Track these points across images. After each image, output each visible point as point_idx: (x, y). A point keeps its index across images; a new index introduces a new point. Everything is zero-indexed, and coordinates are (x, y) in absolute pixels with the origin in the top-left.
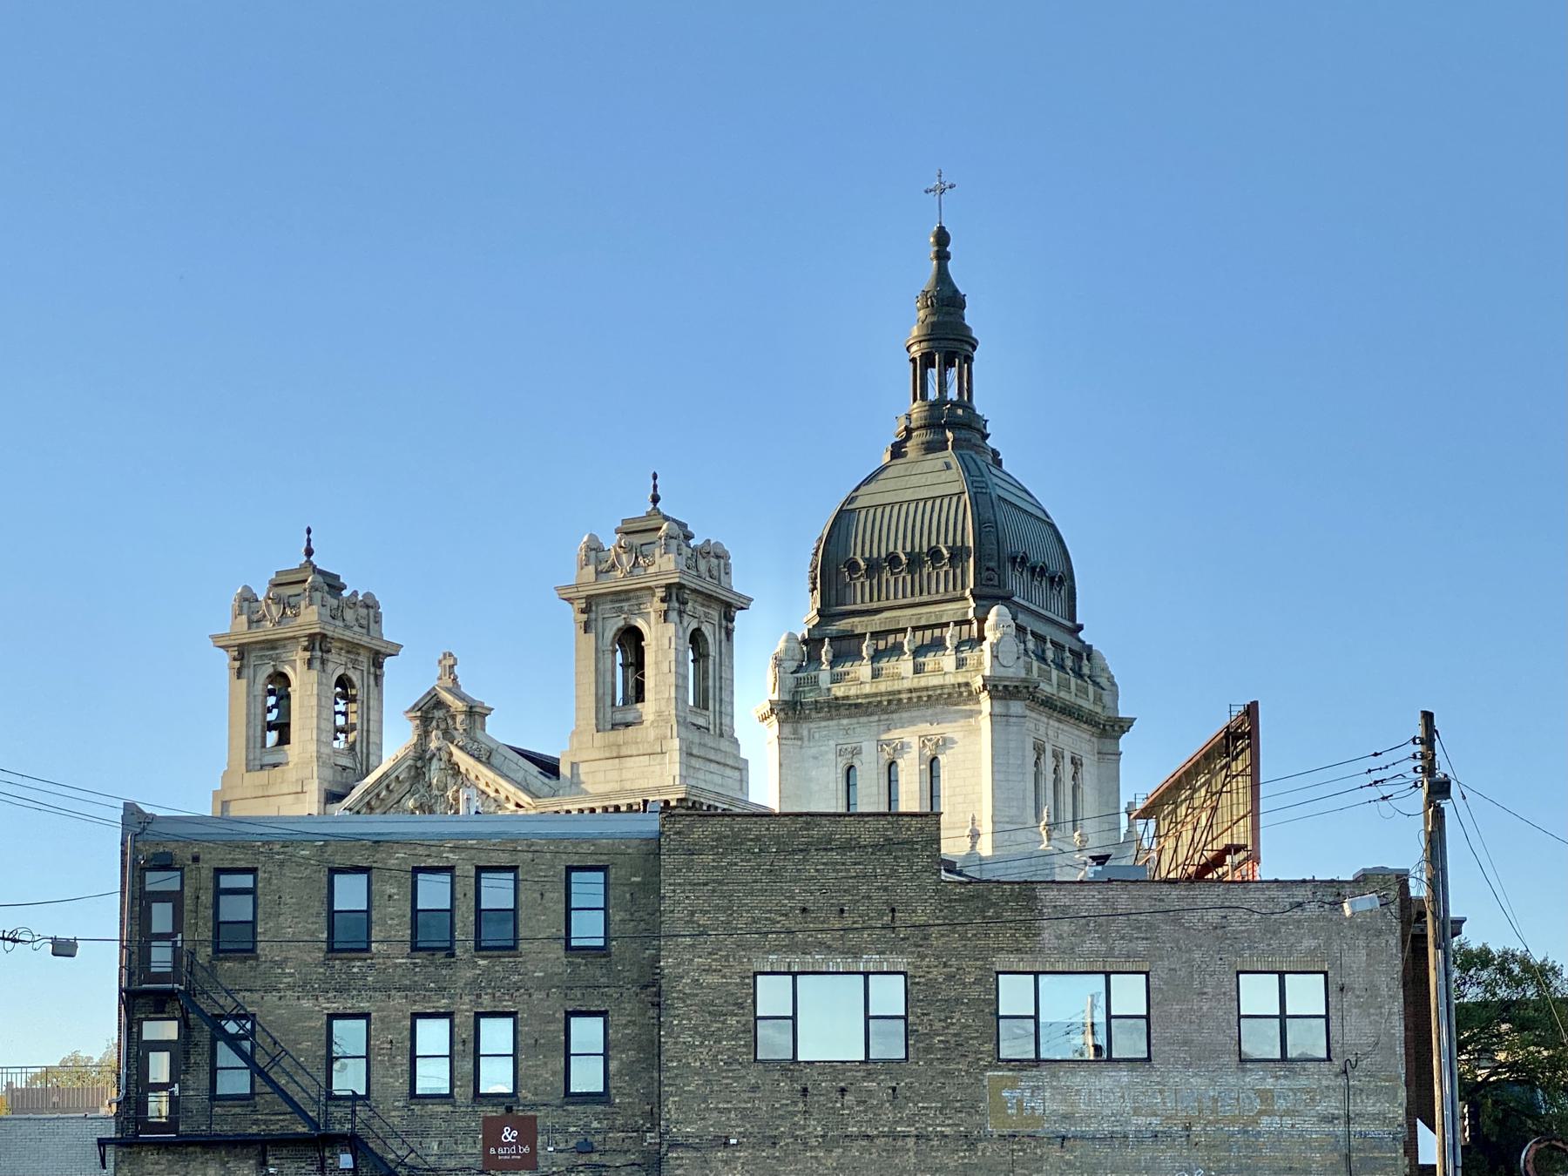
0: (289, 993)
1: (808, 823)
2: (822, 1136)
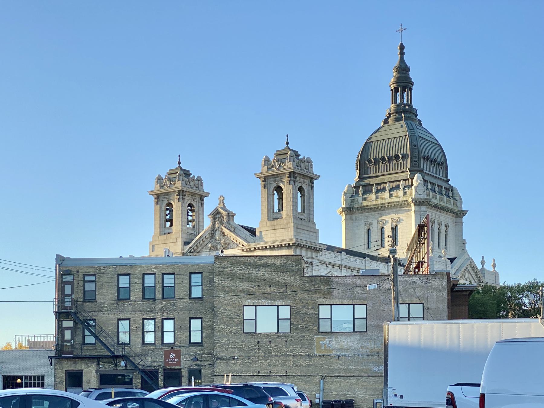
0: (106, 312)
2: (264, 356)
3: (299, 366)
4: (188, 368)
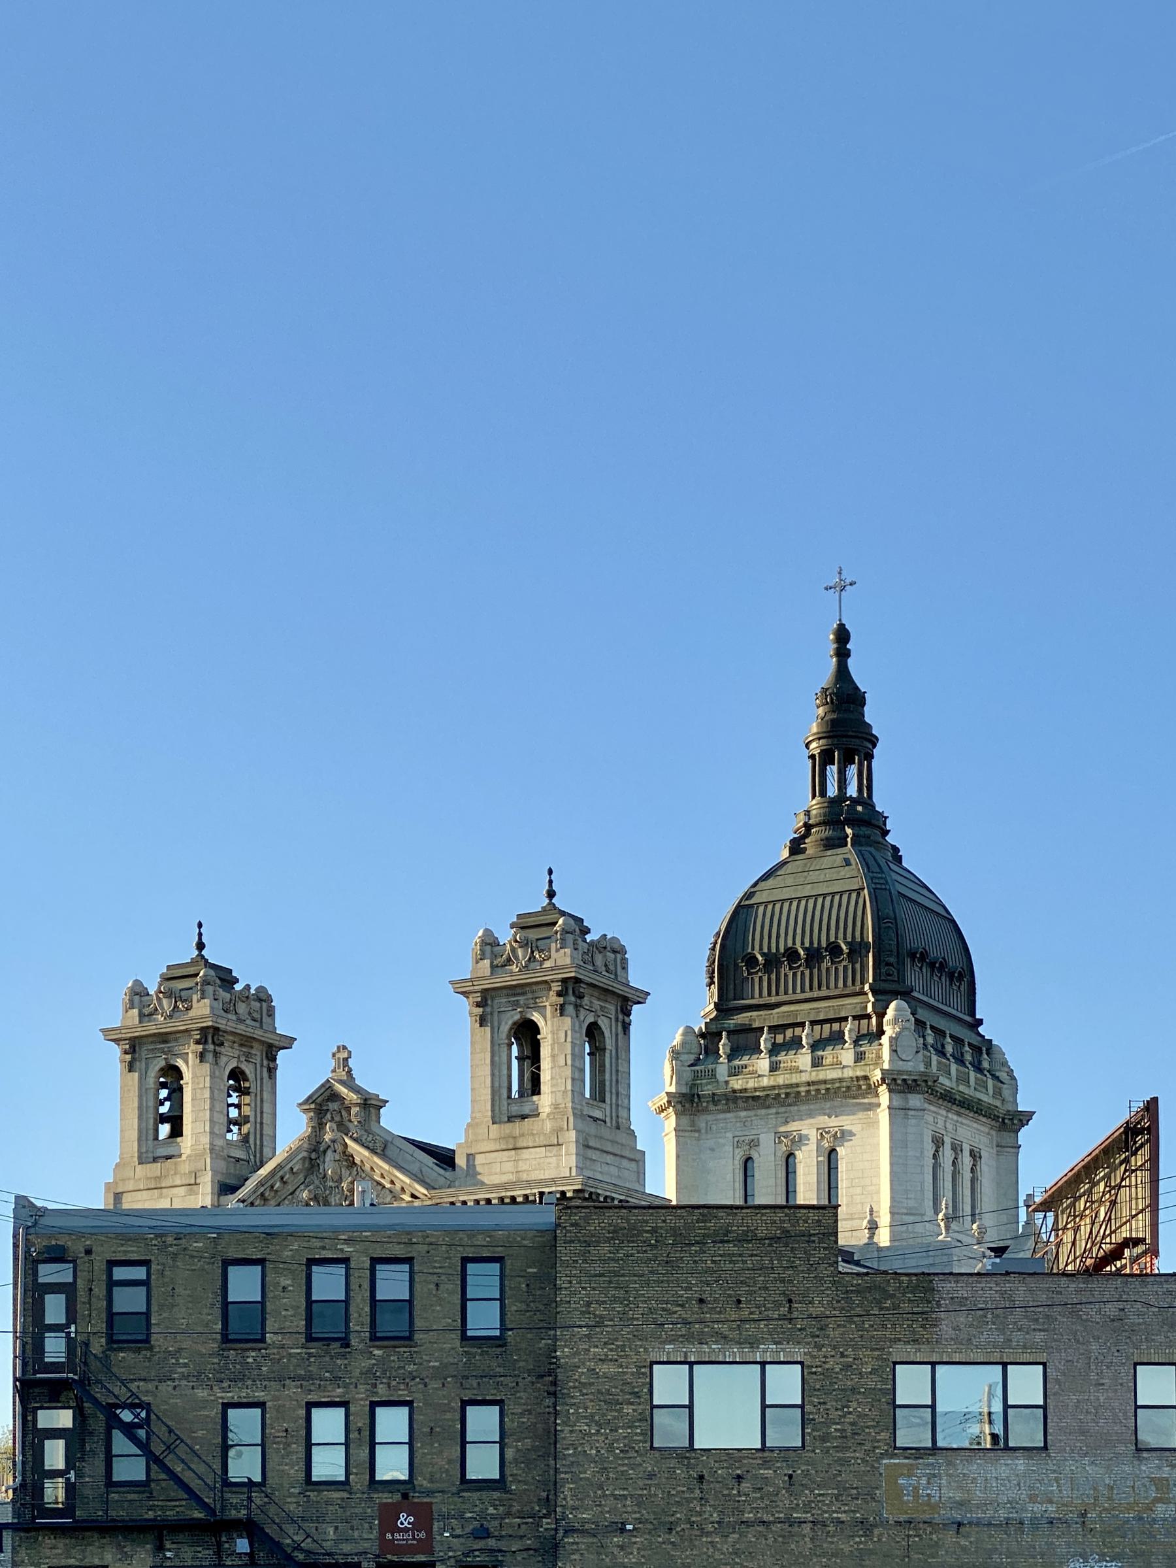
2: (718, 1522)
4: (456, 1561)
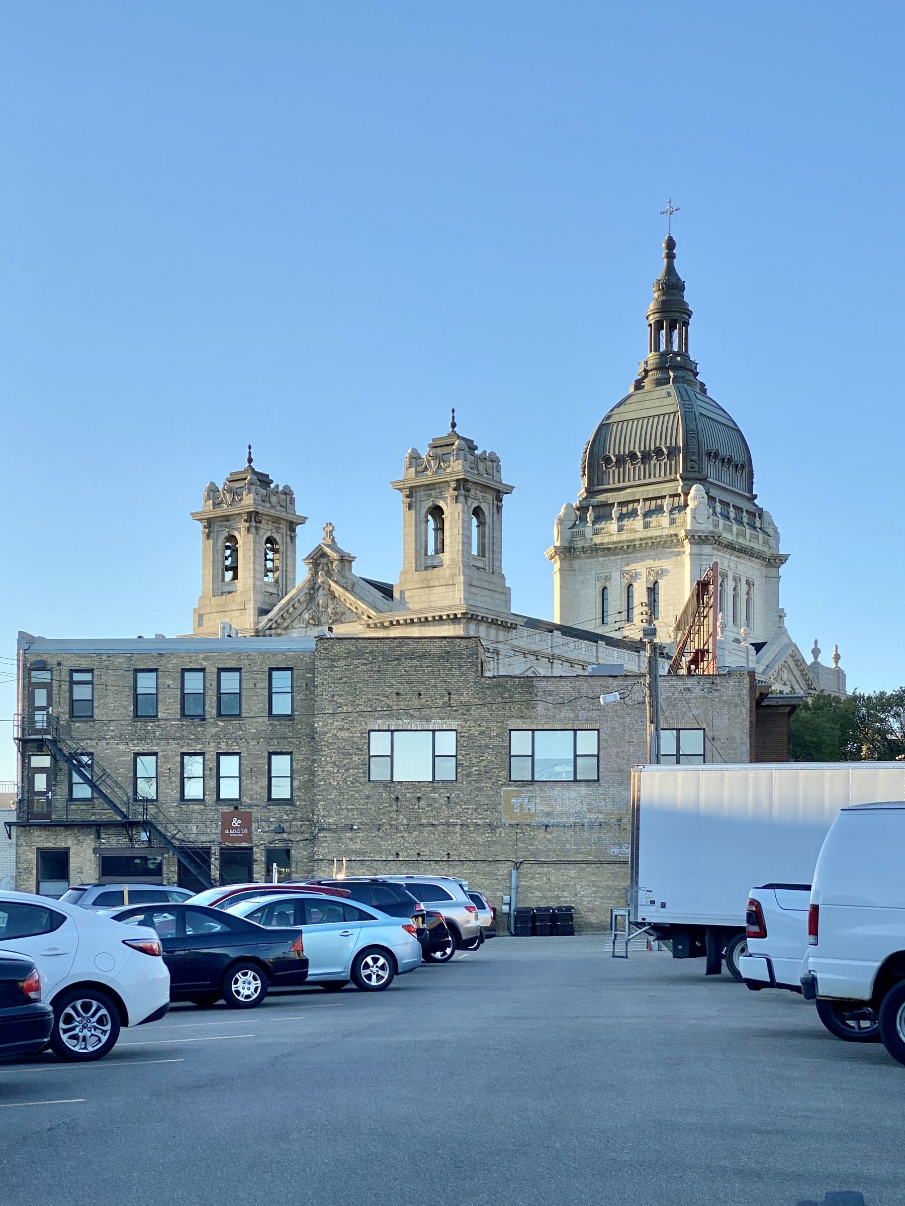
0: (112, 741)
1: (400, 643)
2: (406, 825)
3: (473, 844)
4: (265, 846)
